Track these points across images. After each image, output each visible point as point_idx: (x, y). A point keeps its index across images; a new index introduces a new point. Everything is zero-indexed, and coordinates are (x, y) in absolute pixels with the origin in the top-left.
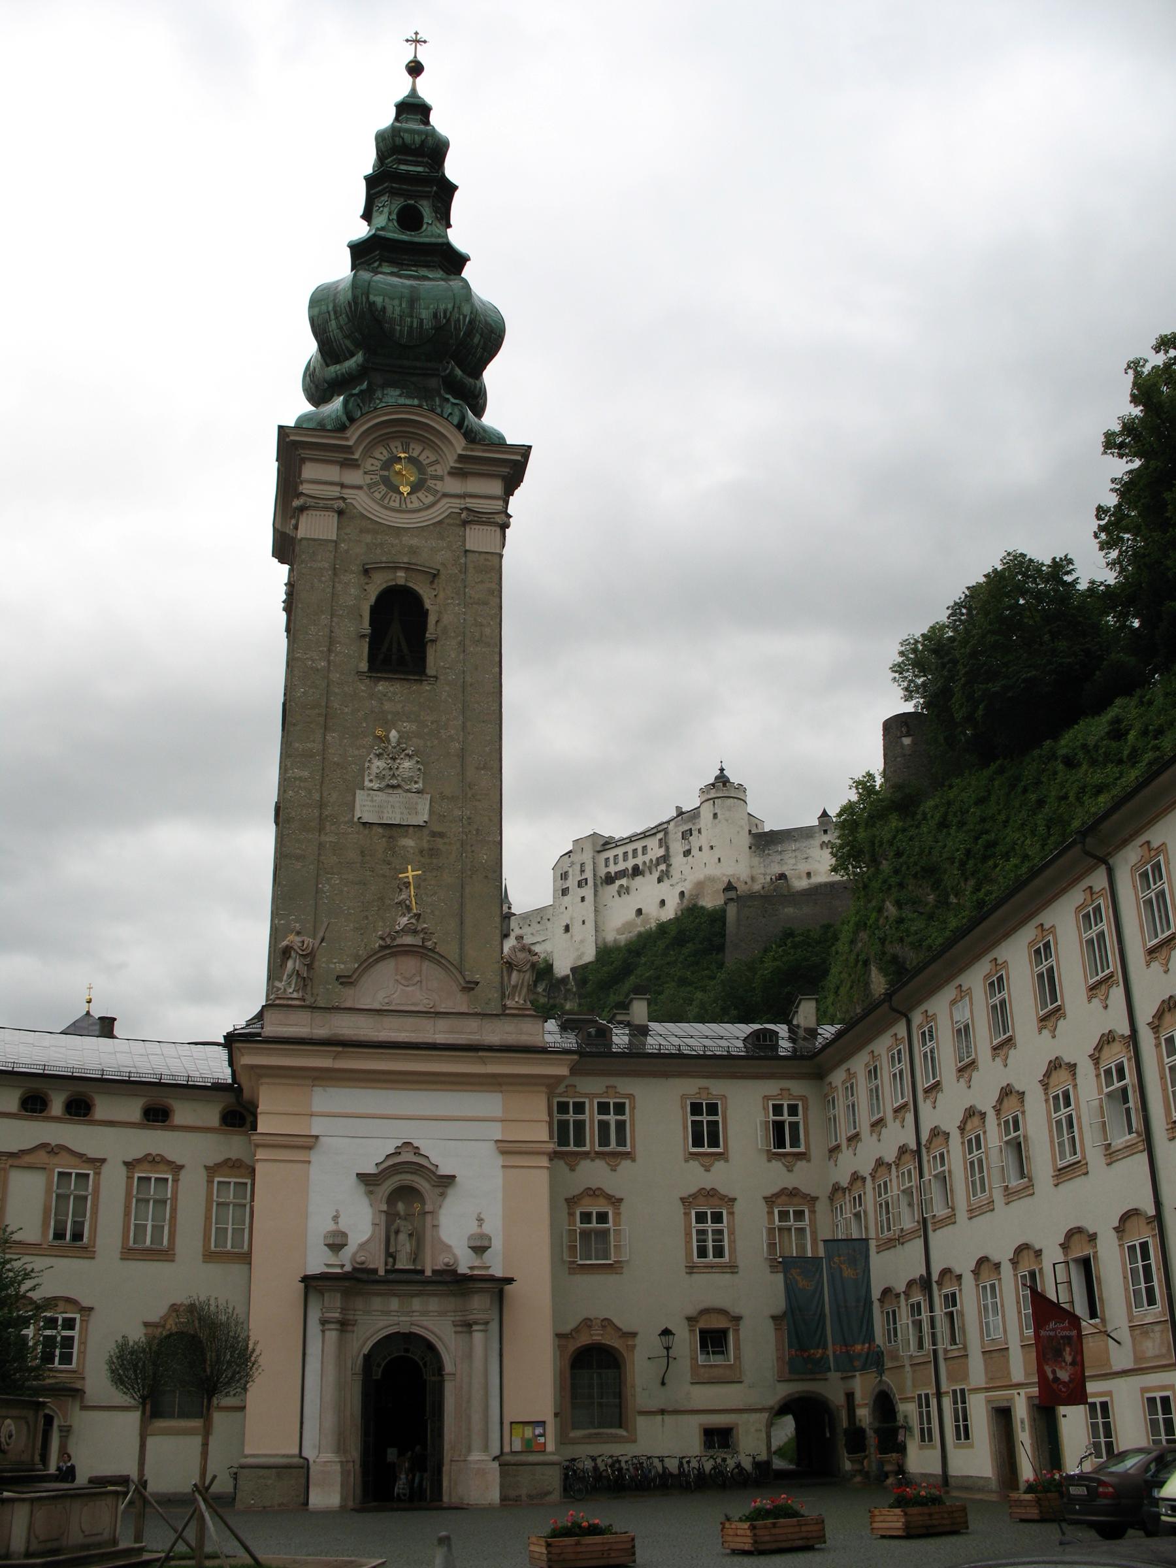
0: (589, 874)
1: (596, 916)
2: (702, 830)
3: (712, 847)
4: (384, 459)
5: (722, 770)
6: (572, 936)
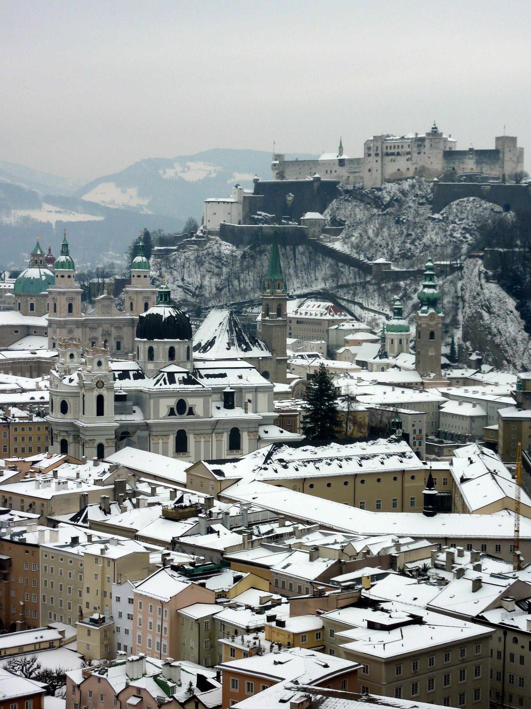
0: (379, 152)
5: (434, 125)
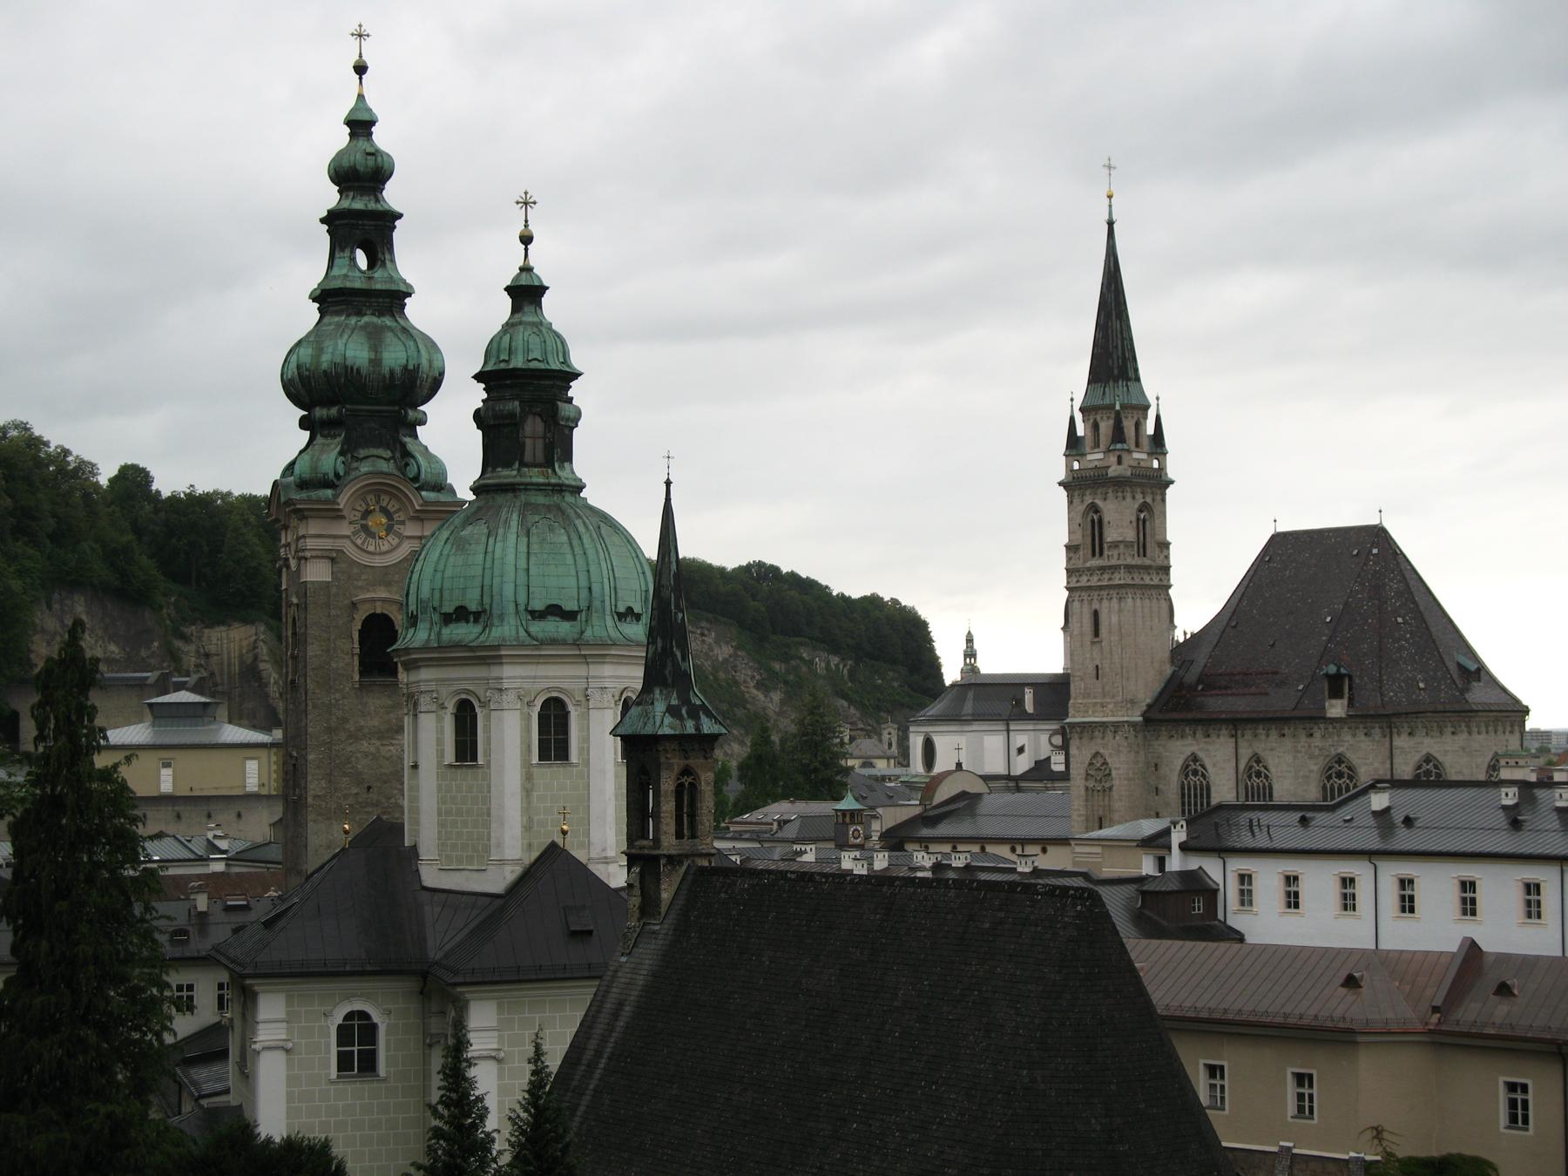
4: (362, 510)
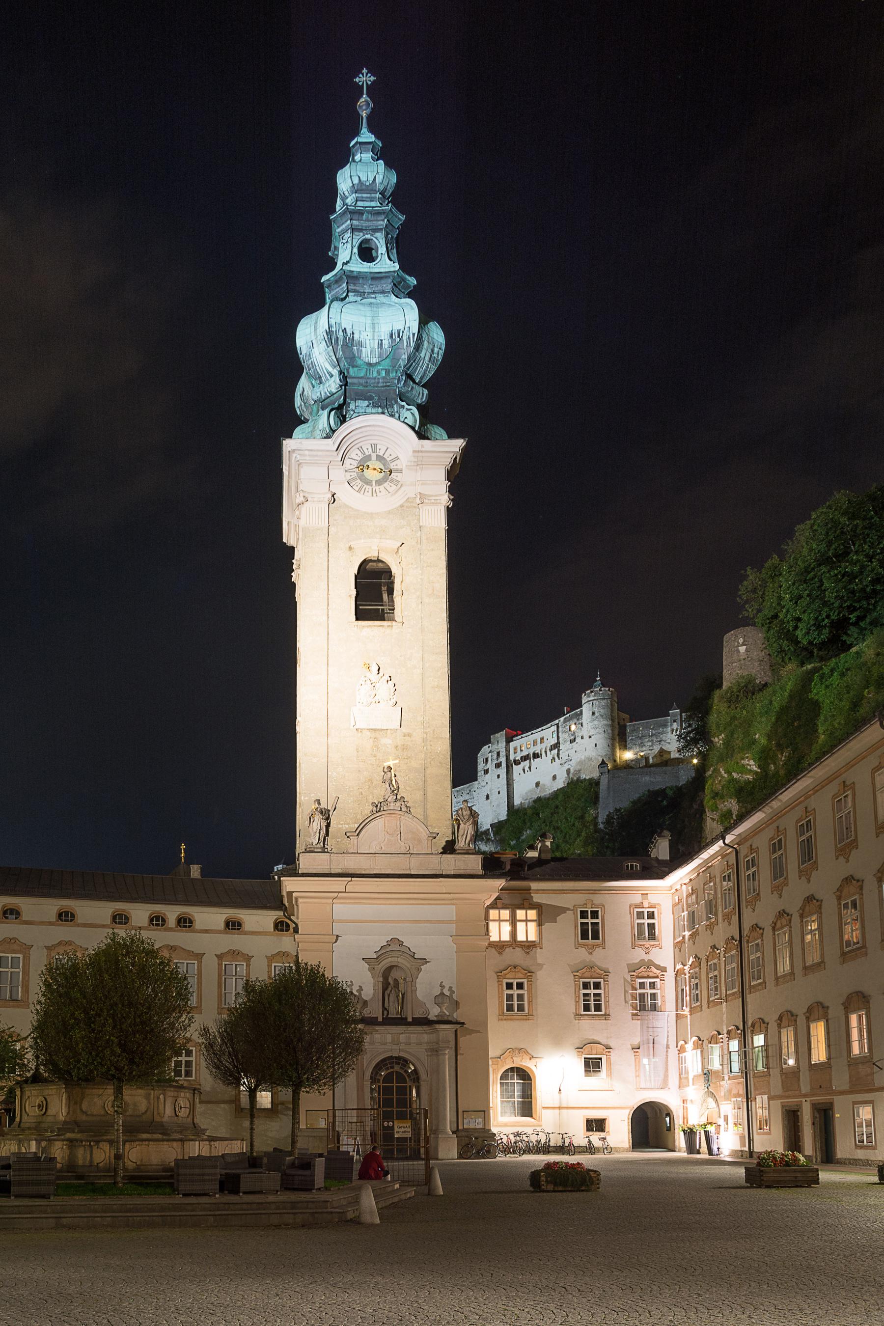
0: (503, 760)
1: (507, 787)
2: (584, 724)
3: (590, 737)
6: (491, 803)
